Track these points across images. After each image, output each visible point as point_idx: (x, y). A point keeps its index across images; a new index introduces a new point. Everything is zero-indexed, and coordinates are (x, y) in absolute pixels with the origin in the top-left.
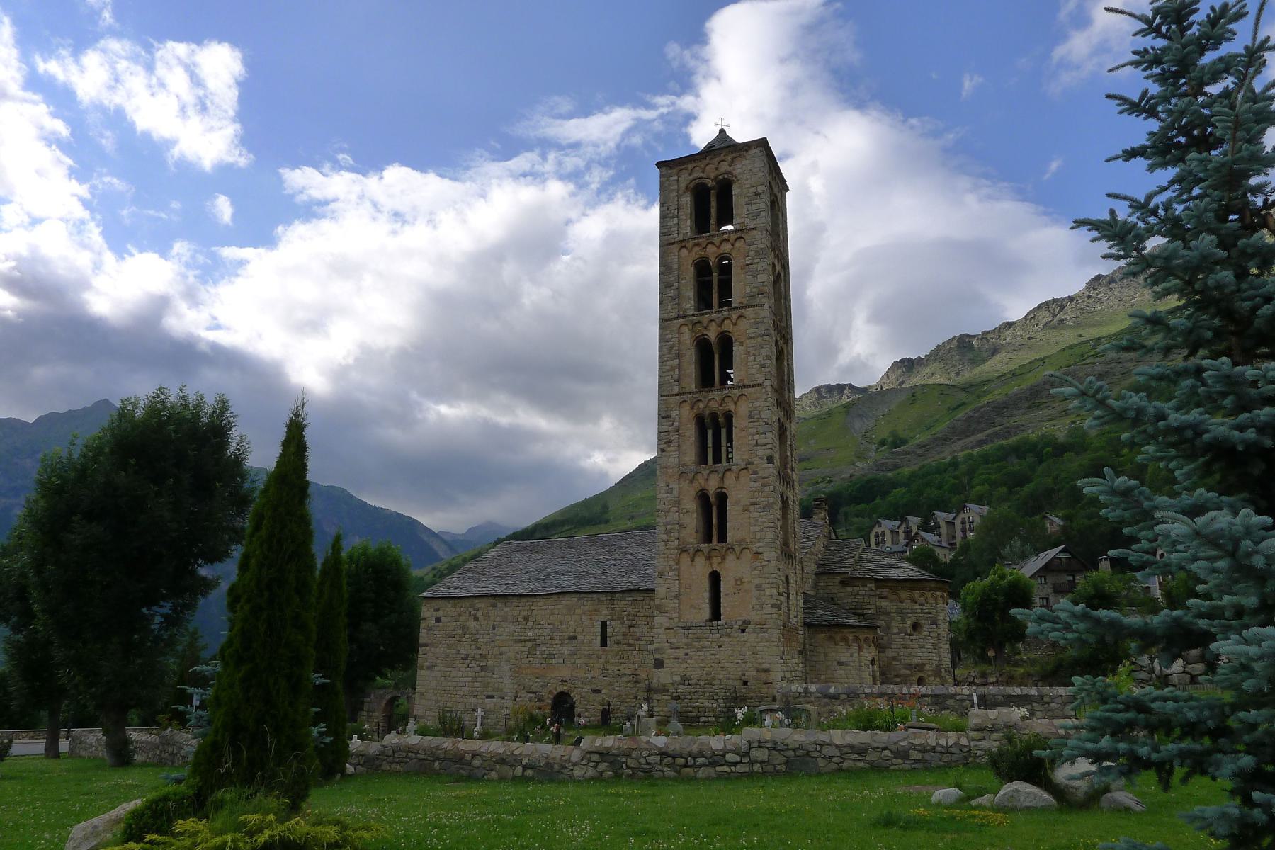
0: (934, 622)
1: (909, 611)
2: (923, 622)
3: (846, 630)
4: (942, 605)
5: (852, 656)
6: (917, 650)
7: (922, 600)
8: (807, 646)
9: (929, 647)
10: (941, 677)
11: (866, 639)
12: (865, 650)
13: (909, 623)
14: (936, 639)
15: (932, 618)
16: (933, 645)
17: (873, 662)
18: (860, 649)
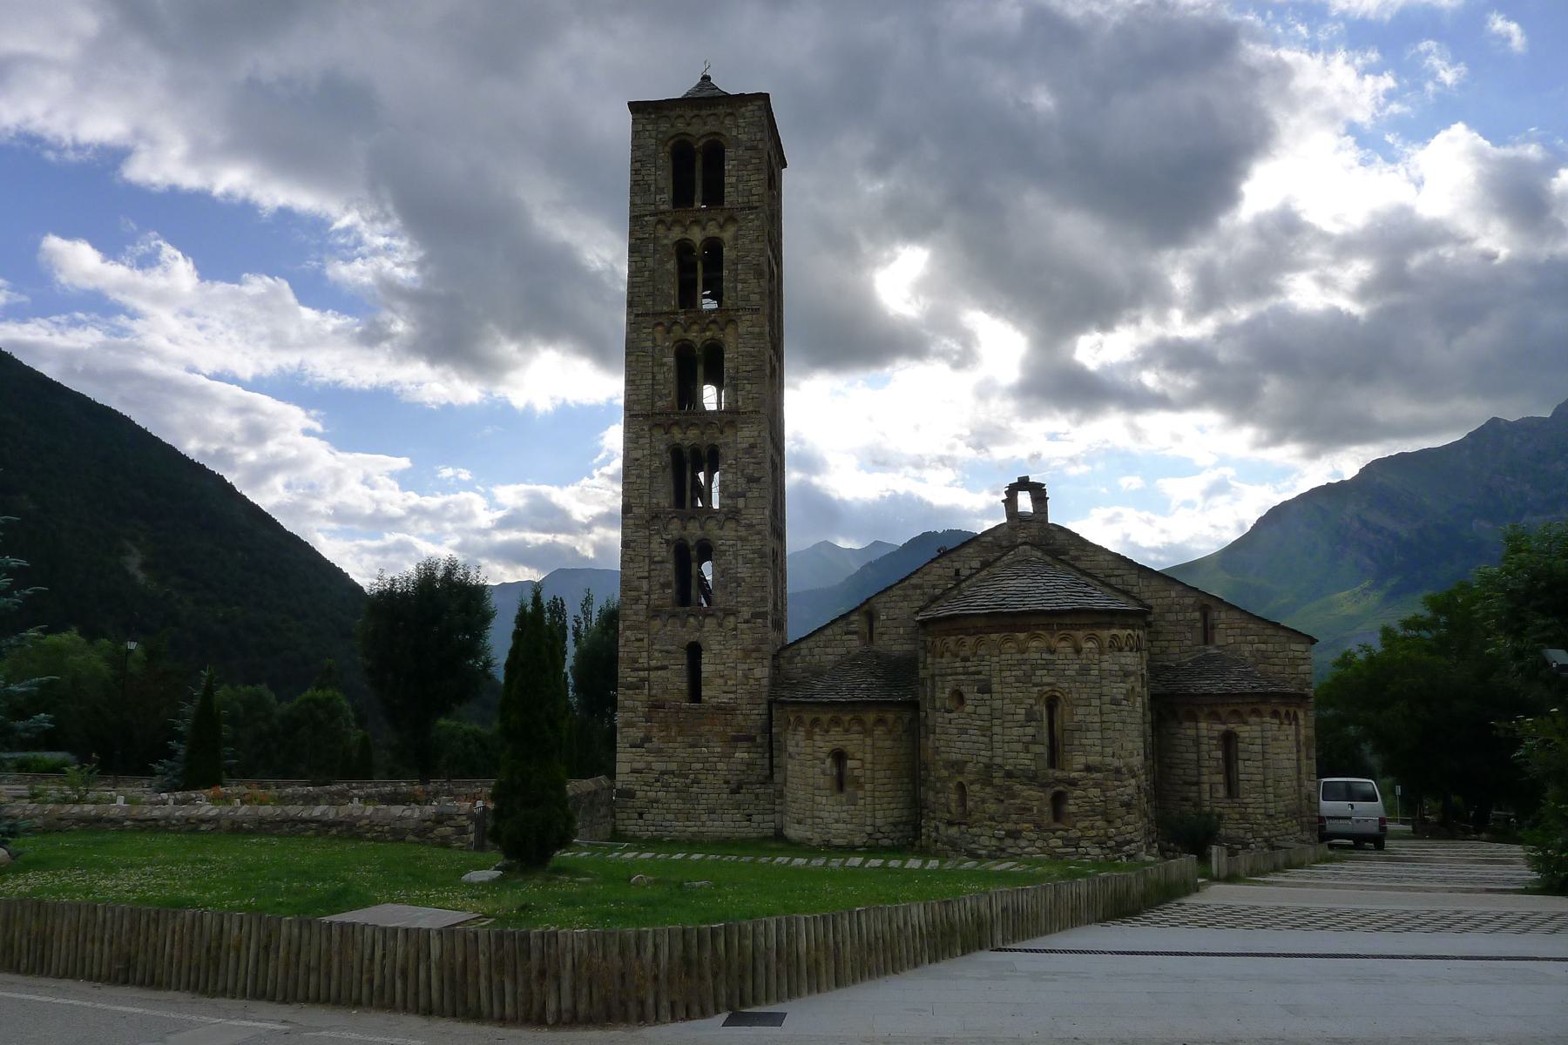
0: (985, 689)
1: (949, 671)
2: (964, 689)
3: (788, 708)
4: (1018, 656)
5: (797, 746)
6: (955, 738)
7: (966, 652)
8: (774, 730)
9: (971, 732)
10: (991, 784)
11: (815, 722)
12: (817, 737)
13: (947, 690)
14: (986, 717)
15: (978, 680)
16: (980, 728)
17: (839, 756)
18: (810, 735)
